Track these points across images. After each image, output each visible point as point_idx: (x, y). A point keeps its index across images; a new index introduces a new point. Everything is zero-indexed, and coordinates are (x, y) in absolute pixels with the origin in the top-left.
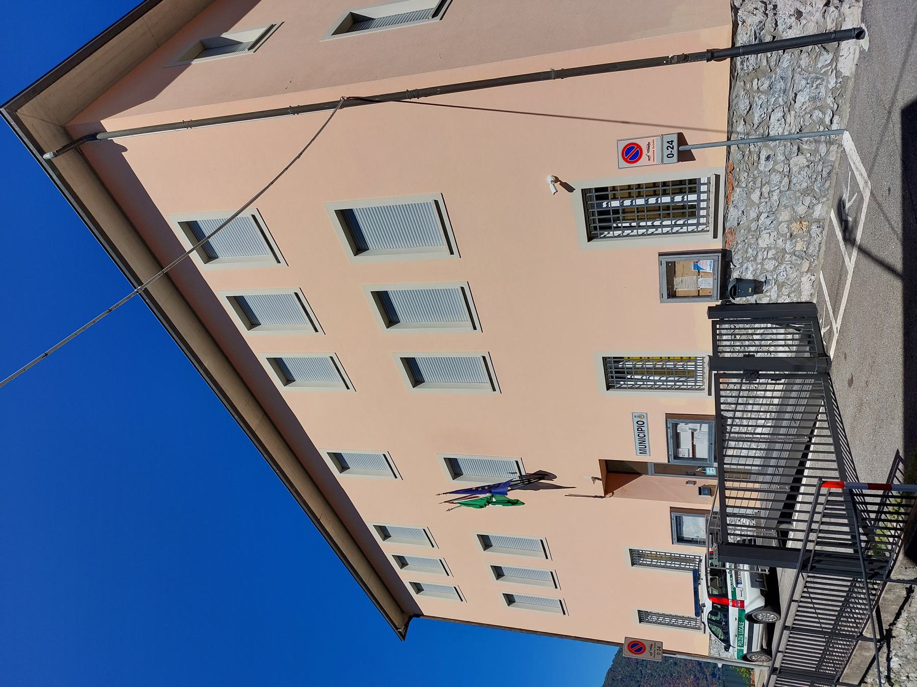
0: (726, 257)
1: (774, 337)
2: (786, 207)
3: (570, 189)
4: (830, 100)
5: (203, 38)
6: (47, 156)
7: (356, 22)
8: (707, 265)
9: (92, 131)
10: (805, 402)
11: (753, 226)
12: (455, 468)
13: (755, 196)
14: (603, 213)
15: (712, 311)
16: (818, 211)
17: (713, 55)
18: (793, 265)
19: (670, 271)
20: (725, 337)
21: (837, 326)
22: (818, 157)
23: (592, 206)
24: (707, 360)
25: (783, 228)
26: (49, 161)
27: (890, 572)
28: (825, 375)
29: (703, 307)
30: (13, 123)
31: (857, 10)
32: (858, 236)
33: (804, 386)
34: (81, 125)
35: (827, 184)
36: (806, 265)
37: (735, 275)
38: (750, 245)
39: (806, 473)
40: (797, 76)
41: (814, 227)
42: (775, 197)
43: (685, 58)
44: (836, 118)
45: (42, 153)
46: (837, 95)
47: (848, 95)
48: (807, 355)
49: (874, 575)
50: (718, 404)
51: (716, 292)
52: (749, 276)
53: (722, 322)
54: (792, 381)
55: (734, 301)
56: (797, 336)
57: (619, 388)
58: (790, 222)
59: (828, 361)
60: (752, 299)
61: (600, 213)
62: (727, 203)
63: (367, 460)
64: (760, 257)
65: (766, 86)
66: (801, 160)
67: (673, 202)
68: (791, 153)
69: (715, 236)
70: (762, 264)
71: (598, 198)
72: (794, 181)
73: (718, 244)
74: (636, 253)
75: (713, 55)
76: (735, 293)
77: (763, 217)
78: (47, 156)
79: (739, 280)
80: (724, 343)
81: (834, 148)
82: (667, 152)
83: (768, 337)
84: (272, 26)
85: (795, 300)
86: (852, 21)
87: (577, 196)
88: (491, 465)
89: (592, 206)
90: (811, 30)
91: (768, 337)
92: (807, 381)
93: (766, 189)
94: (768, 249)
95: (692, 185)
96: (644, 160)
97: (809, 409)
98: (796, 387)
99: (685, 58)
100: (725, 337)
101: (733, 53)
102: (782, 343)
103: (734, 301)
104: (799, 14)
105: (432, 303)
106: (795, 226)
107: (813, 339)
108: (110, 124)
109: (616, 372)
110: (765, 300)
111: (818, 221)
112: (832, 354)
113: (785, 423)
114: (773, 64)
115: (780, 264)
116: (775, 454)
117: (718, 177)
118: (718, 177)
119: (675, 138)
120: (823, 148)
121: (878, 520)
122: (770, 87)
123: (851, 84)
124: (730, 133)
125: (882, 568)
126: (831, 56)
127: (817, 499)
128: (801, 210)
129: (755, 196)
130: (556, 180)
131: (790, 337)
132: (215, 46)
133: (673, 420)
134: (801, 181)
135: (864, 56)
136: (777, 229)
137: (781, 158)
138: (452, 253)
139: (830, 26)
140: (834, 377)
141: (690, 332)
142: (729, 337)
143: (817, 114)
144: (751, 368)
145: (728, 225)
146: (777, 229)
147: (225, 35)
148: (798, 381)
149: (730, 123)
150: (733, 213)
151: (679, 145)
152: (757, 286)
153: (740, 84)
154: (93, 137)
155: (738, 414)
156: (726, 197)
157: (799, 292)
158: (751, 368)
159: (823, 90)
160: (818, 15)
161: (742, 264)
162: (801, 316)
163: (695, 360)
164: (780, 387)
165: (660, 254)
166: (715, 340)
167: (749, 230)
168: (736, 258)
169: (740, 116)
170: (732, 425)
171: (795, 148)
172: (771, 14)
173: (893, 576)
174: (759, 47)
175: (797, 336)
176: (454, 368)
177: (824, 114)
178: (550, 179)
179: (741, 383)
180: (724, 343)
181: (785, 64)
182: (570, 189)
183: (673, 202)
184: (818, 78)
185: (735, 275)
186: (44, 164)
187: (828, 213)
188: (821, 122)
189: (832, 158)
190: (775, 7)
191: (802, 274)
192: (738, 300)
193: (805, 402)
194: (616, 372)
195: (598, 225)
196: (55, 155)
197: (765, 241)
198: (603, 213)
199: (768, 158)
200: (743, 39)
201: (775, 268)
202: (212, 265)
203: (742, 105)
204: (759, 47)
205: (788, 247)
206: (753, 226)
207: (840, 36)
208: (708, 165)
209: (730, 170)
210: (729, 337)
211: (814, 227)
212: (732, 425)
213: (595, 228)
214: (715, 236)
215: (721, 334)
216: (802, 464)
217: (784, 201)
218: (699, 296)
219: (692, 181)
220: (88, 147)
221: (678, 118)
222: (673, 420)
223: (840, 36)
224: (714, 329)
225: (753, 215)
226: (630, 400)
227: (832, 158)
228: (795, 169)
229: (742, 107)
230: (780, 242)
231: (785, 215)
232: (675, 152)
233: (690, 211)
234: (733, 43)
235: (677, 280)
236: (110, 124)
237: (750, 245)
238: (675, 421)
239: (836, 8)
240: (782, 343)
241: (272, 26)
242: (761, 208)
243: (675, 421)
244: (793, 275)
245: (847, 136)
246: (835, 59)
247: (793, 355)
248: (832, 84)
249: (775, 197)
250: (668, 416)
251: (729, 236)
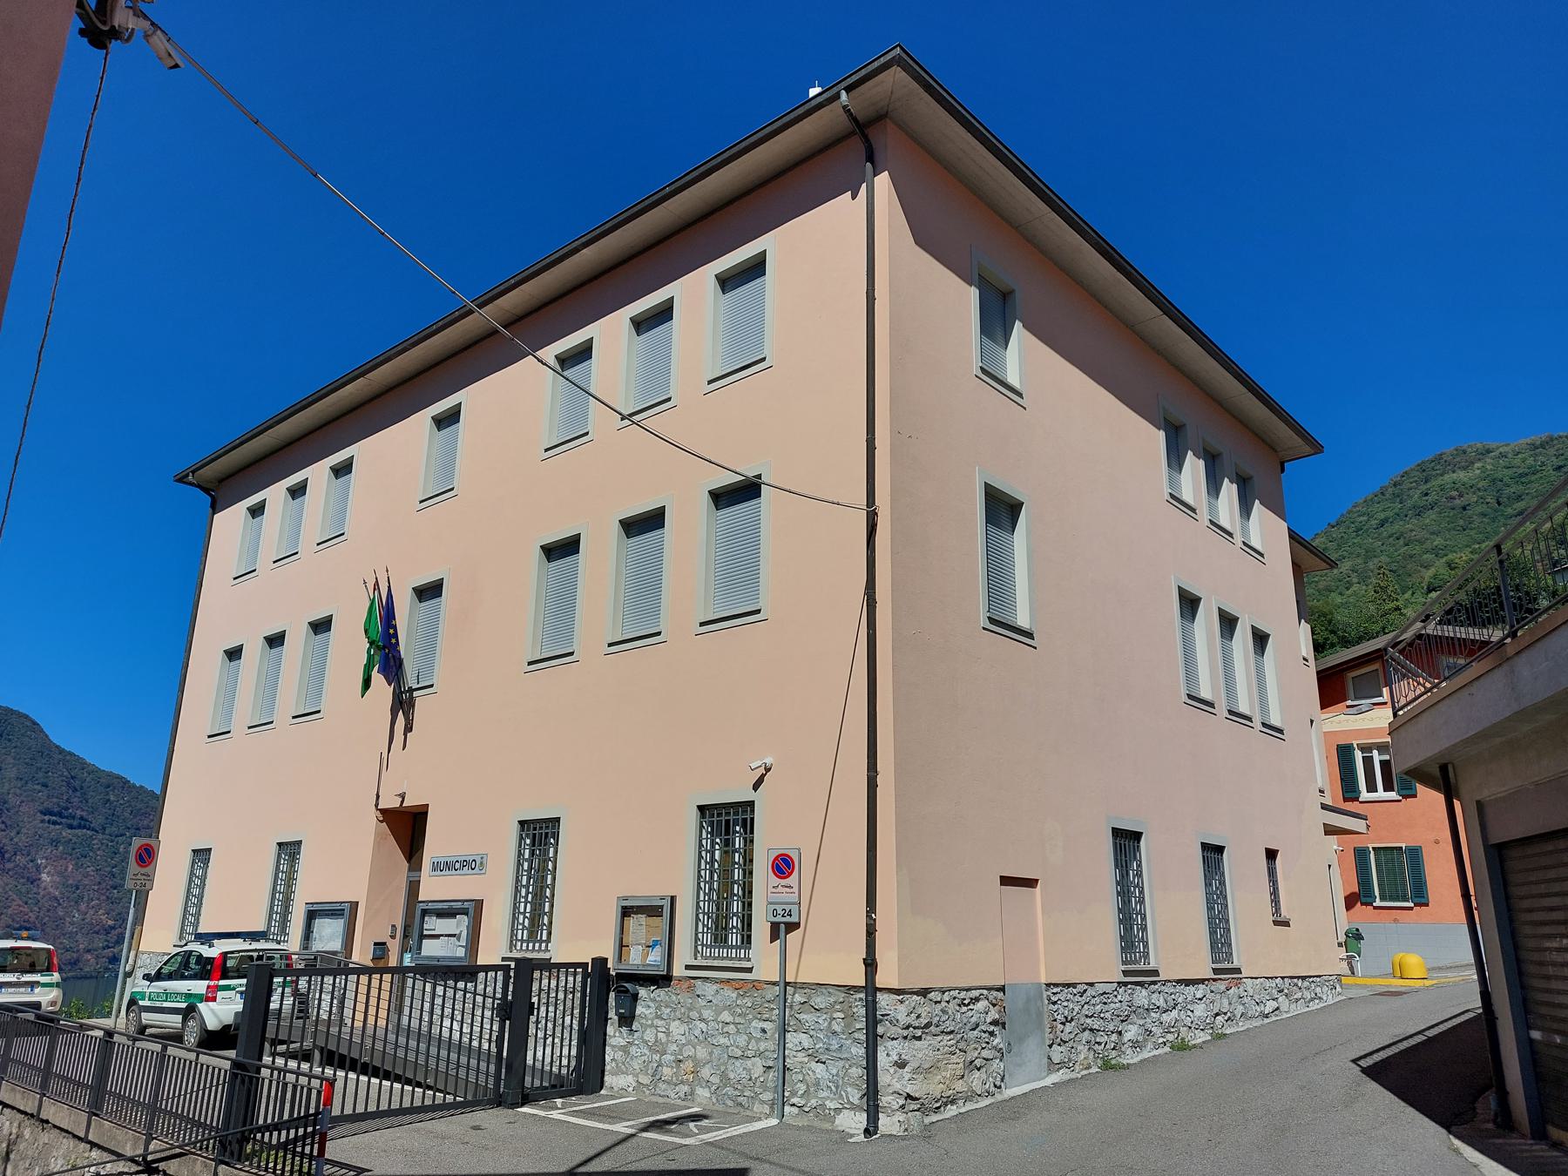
0: (662, 980)
1: (566, 1042)
2: (711, 1054)
3: (756, 787)
4: (813, 1102)
5: (1018, 295)
6: (844, 95)
7: (1002, 510)
8: (655, 957)
9: (878, 156)
10: (472, 1079)
11: (694, 1014)
12: (429, 592)
13: (726, 1016)
14: (727, 823)
15: (601, 962)
16: (703, 1093)
17: (870, 964)
18: (646, 1064)
19: (652, 911)
20: (571, 979)
21: (555, 1114)
22: (758, 1090)
23: (736, 813)
24: (547, 956)
25: (689, 1051)
26: (837, 96)
27: (227, 1164)
28: (499, 1101)
29: (608, 951)
30: (882, 60)
31: (896, 1130)
32: (645, 1135)
33: (485, 1075)
34: (888, 140)
35: (730, 1103)
36: (645, 1080)
37: (643, 992)
38: (674, 1010)
39: (375, 1081)
40: (841, 1063)
41: (686, 1088)
42: (723, 1040)
43: (871, 932)
44: (795, 1110)
45: (848, 89)
46: (820, 1111)
47: (817, 1123)
48: (528, 1084)
49: (223, 1145)
50: (487, 969)
51: (624, 968)
52: (639, 1010)
53: (585, 975)
54: (493, 1060)
55: (609, 990)
56: (564, 1071)
57: (521, 838)
58: (693, 1058)
59: (514, 1105)
60: (612, 1014)
61: (728, 822)
62: (722, 981)
63: (447, 463)
64: (660, 1023)
65: (836, 1027)
66: (758, 1071)
67: (727, 917)
68: (767, 1058)
69: (688, 967)
70: (652, 1026)
71: (745, 820)
72: (738, 1063)
73: (678, 971)
74: (674, 868)
75: (870, 964)
76: (621, 992)
77: (703, 1026)
78: (844, 95)
79: (635, 997)
80: (563, 978)
81: (767, 1109)
82: (779, 908)
83: (566, 1035)
84: (1020, 395)
85: (608, 1068)
86: (886, 1124)
87: (746, 795)
88: (429, 649)
89: (736, 813)
90: (883, 1079)
91: (566, 1035)
92: (491, 1081)
93: (731, 1029)
94: (668, 1033)
95: (747, 940)
96: (775, 880)
97: (461, 1084)
98: (483, 1065)
99: (871, 932)
100: (571, 979)
101: (871, 989)
102: (551, 1049)
103: (609, 990)
104: (901, 1065)
105: (645, 588)
106: (689, 1065)
107: (559, 1088)
108: (883, 181)
109: (540, 835)
110: (610, 1030)
111: (692, 1093)
112: (524, 1109)
113: (454, 1056)
114: (856, 1035)
115: (650, 1048)
116: (413, 1044)
117: (750, 970)
118: (750, 970)
119: (794, 919)
120: (767, 1096)
121: (294, 1154)
122: (834, 1033)
123: (827, 1126)
124: (795, 985)
125: (232, 1154)
126: (856, 1102)
127: (316, 1077)
128: (706, 1072)
129: (726, 1016)
130: (768, 770)
131: (565, 1062)
132: (997, 317)
133: (473, 910)
134: (737, 1071)
135: (844, 1136)
136: (689, 1042)
137: (762, 1046)
138: (702, 624)
139: (885, 1100)
140: (496, 1111)
141: (581, 936)
142: (570, 985)
143: (802, 1088)
144: (515, 1012)
145: (699, 982)
146: (689, 1042)
147: (1018, 325)
148: (492, 1068)
149: (804, 986)
150: (710, 989)
151: (786, 924)
152: (627, 1020)
153: (841, 996)
154: (870, 158)
155: (479, 999)
156: (728, 981)
157: (614, 1074)
158: (515, 1012)
159: (825, 1094)
160: (898, 1086)
161: (653, 1000)
162: (586, 1077)
163: (548, 940)
164: (485, 1046)
165: (673, 899)
166: (567, 965)
167: (690, 1009)
168: (661, 994)
169: (810, 998)
170: (455, 989)
171: (770, 1063)
172: (905, 1033)
173: (222, 1168)
174: (873, 1020)
175: (564, 1071)
176: (561, 608)
177: (802, 1096)
178: (769, 761)
179: (494, 998)
180: (563, 978)
181: (854, 1050)
182: (756, 787)
183: (727, 917)
184: (837, 1088)
185: (643, 992)
186: (835, 90)
187: (699, 1105)
188: (794, 1094)
189: (757, 1108)
190: (919, 1039)
191: (636, 1076)
192: (612, 995)
193: (472, 1079)
194: (540, 835)
195: (723, 818)
196: (844, 107)
197: (677, 1028)
198: (727, 823)
199: (764, 1031)
200: (883, 1000)
201: (646, 1042)
202: (712, 284)
203: (819, 1001)
204: (873, 1020)
205: (668, 1057)
206: (694, 1014)
207: (873, 1111)
208: (764, 959)
209: (756, 985)
210: (570, 985)
211: (686, 1088)
212: (455, 989)
213: (719, 815)
214: (688, 967)
215: (575, 974)
216: (398, 1078)
217: (717, 1051)
218: (622, 946)
219: (749, 942)
220: (857, 144)
221: (816, 925)
222: (473, 910)
223: (873, 1111)
224: (575, 965)
225: (707, 1014)
226: (504, 852)
227: (757, 1108)
228: (749, 1063)
229: (818, 1000)
230: (674, 1047)
231: (702, 1053)
232: (779, 919)
233: (720, 939)
234: (881, 990)
235: (642, 918)
236: (883, 181)
237: (674, 1010)
238: (471, 912)
239: (903, 1107)
240: (551, 1049)
241: (1020, 395)
242: (712, 1024)
243: (471, 912)
244: (636, 1065)
245: (774, 1122)
246: (854, 1108)
247: (530, 1061)
248: (829, 1104)
249: (723, 1040)
250: (479, 904)
251: (686, 985)
